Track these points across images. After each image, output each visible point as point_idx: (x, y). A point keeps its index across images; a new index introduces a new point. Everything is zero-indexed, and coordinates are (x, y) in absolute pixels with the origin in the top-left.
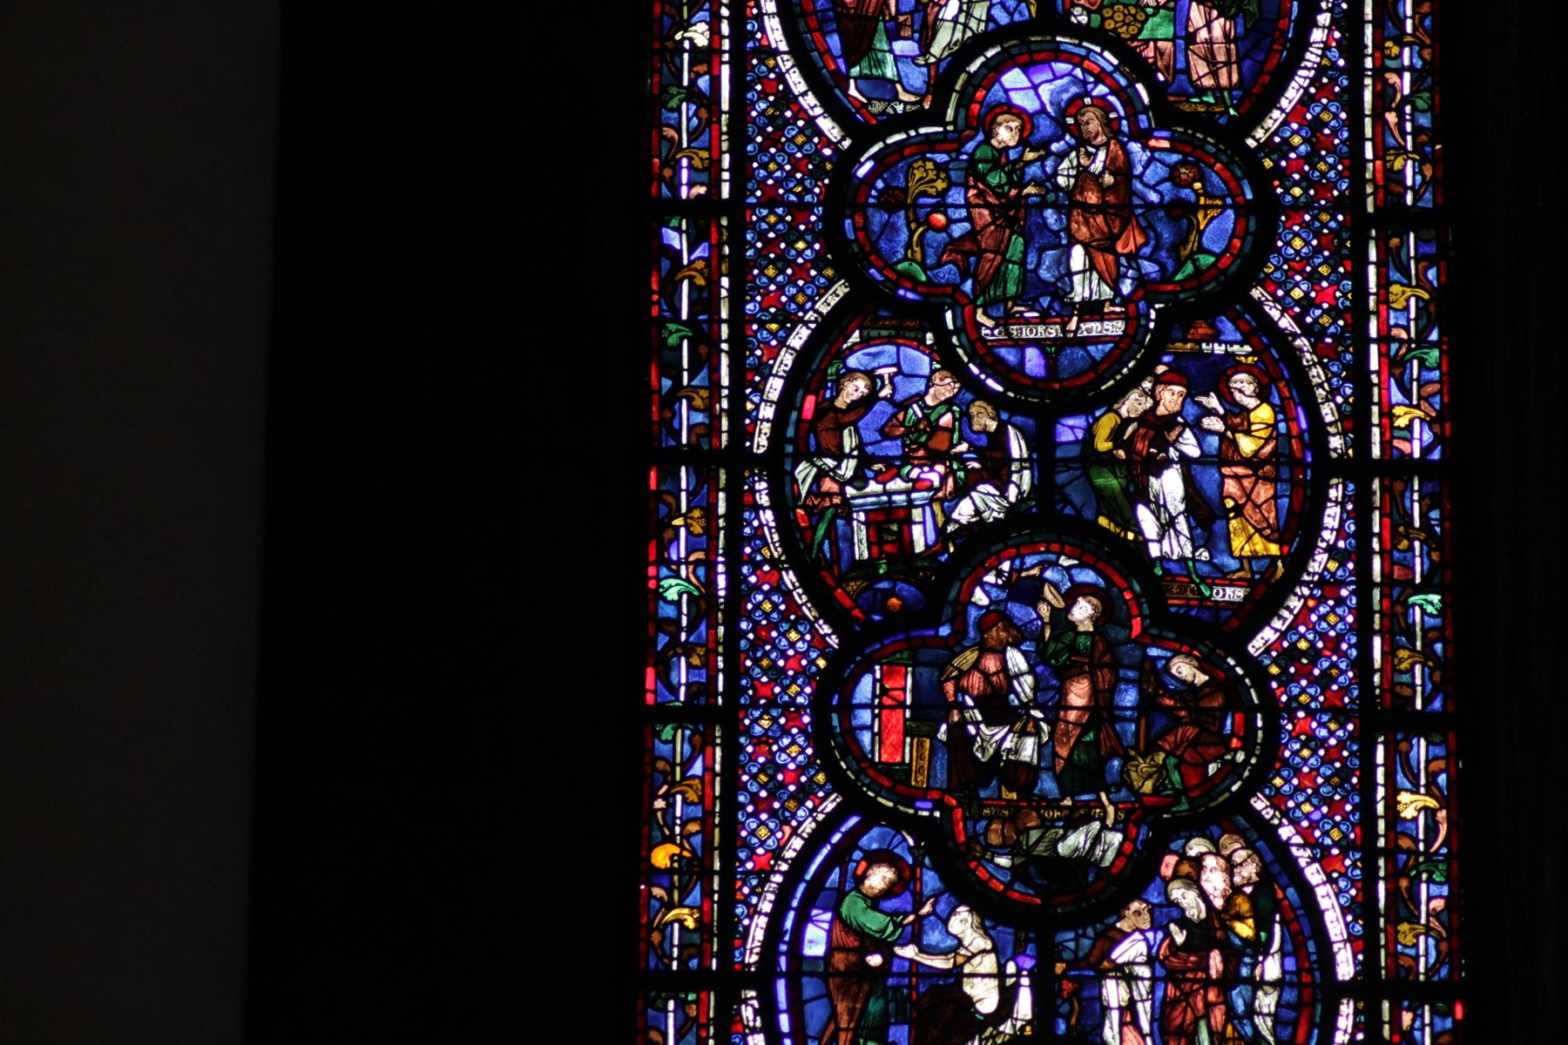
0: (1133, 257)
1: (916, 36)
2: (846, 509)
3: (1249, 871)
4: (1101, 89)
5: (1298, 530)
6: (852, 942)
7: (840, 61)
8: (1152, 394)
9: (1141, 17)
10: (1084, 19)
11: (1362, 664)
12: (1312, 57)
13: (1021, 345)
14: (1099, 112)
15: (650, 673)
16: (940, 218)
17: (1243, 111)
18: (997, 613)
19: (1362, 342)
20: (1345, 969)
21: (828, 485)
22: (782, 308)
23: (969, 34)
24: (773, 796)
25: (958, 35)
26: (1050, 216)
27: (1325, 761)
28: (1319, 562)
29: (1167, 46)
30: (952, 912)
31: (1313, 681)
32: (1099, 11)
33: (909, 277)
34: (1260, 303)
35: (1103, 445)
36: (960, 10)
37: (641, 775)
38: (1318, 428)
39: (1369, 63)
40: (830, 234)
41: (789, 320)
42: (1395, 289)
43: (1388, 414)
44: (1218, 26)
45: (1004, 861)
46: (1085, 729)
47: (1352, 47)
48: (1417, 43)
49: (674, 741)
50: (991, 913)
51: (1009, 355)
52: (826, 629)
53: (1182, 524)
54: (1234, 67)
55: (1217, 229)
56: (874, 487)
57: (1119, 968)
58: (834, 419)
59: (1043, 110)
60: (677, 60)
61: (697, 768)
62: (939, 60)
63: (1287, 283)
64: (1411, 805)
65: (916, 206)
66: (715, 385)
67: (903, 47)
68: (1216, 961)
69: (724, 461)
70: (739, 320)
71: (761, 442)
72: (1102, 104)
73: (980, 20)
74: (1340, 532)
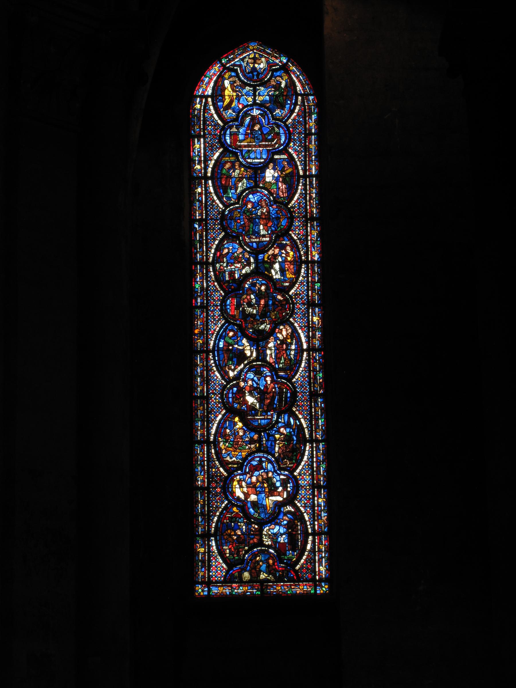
0: (270, 227)
2: (225, 271)
3: (290, 331)
4: (265, 198)
5: (297, 273)
6: (227, 345)
8: (274, 250)
11: (308, 295)
12: (299, 191)
13: (252, 242)
15: (194, 301)
16: (239, 221)
18: (249, 289)
19: (307, 241)
20: (305, 346)
21: (222, 268)
22: (214, 237)
24: (214, 320)
26: (257, 220)
27: (302, 312)
28: (301, 278)
30: (243, 339)
31: (300, 299)
33: (234, 231)
34: (291, 234)
35: (266, 259)
37: (193, 318)
38: (301, 256)
40: (221, 224)
41: (215, 239)
42: (313, 231)
43: (311, 253)
44: (284, 186)
45: (251, 330)
46: (263, 308)
47: (305, 189)
48: (316, 188)
49: (198, 312)
50: (249, 339)
51: (251, 244)
52: (222, 292)
53: (279, 273)
55: (284, 222)
56: (229, 268)
57: (269, 348)
58: (222, 256)
61: (202, 317)
63: (295, 231)
64: (315, 319)
65: (235, 219)
66: (203, 251)
67: (232, 191)
68: (284, 346)
69: (205, 264)
70: (207, 240)
71: (211, 260)
74: (304, 273)
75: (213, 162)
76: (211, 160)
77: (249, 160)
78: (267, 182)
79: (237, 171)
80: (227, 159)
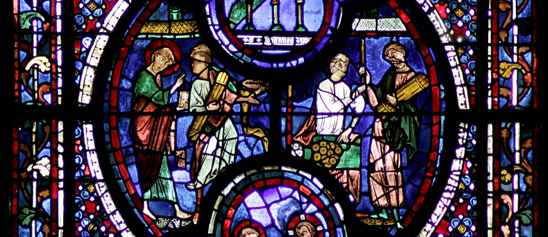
1: (188, 166)
4: (312, 208)
7: (138, 187)
9: (338, 151)
10: (300, 153)
12: (452, 182)
14: (310, 226)
17: (407, 223)
23: (223, 165)
25: (216, 166)
29: (355, 173)
32: (310, 147)
36: (218, 146)
39: (490, 187)
47: (479, 175)
54: (401, 190)
59: (273, 225)
60: (29, 187)
62: (204, 186)
67: (181, 175)
72: (312, 219)
73: (231, 154)
75: (102, 41)
76: (93, 33)
77: (249, 40)
78: (322, 138)
79: (201, 86)
80: (160, 29)
